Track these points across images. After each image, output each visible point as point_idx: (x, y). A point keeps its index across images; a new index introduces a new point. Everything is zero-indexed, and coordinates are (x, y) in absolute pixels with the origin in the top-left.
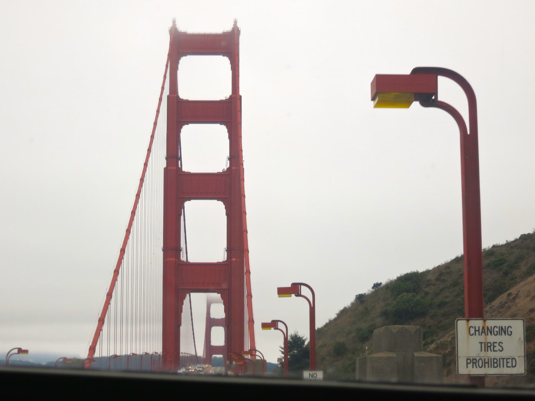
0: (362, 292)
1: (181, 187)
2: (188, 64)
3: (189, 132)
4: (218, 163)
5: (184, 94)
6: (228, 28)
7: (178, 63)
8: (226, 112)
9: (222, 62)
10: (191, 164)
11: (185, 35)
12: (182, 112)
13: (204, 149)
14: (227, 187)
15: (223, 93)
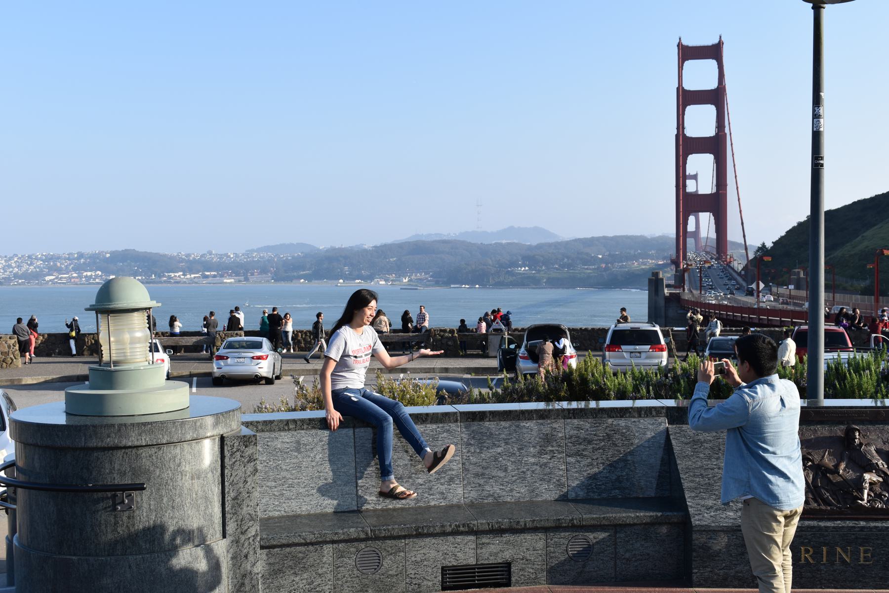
1: (686, 146)
3: (691, 110)
4: (709, 130)
5: (688, 86)
6: (716, 41)
8: (715, 97)
9: (712, 64)
11: (687, 47)
12: (687, 98)
13: (701, 122)
14: (716, 146)
15: (713, 85)
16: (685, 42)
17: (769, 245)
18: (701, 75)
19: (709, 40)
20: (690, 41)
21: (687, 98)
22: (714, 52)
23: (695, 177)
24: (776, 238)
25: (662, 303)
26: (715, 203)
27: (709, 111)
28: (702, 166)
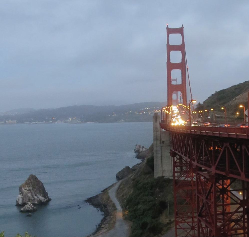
0: (213, 94)
2: (171, 35)
3: (172, 53)
4: (179, 61)
5: (171, 43)
6: (181, 26)
7: (169, 36)
9: (179, 35)
10: (172, 61)
12: (170, 48)
13: (176, 57)
14: (182, 66)
15: (180, 43)
16: (169, 27)
17: (202, 103)
18: (175, 39)
19: (178, 26)
20: (171, 27)
21: (170, 48)
22: (180, 31)
23: (176, 80)
24: (204, 100)
25: (158, 126)
26: (182, 88)
27: (179, 53)
28: (176, 74)
